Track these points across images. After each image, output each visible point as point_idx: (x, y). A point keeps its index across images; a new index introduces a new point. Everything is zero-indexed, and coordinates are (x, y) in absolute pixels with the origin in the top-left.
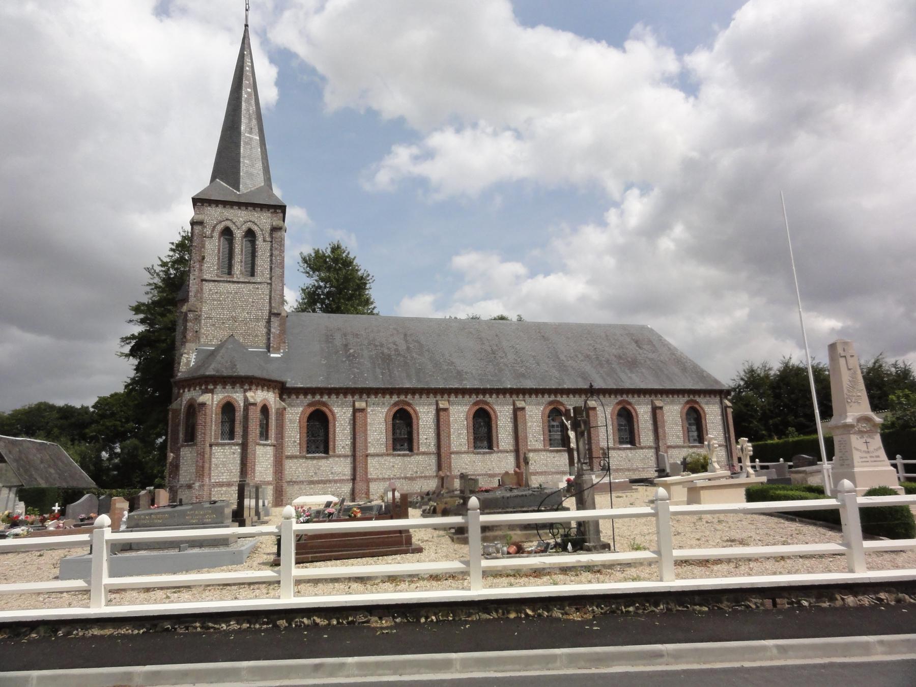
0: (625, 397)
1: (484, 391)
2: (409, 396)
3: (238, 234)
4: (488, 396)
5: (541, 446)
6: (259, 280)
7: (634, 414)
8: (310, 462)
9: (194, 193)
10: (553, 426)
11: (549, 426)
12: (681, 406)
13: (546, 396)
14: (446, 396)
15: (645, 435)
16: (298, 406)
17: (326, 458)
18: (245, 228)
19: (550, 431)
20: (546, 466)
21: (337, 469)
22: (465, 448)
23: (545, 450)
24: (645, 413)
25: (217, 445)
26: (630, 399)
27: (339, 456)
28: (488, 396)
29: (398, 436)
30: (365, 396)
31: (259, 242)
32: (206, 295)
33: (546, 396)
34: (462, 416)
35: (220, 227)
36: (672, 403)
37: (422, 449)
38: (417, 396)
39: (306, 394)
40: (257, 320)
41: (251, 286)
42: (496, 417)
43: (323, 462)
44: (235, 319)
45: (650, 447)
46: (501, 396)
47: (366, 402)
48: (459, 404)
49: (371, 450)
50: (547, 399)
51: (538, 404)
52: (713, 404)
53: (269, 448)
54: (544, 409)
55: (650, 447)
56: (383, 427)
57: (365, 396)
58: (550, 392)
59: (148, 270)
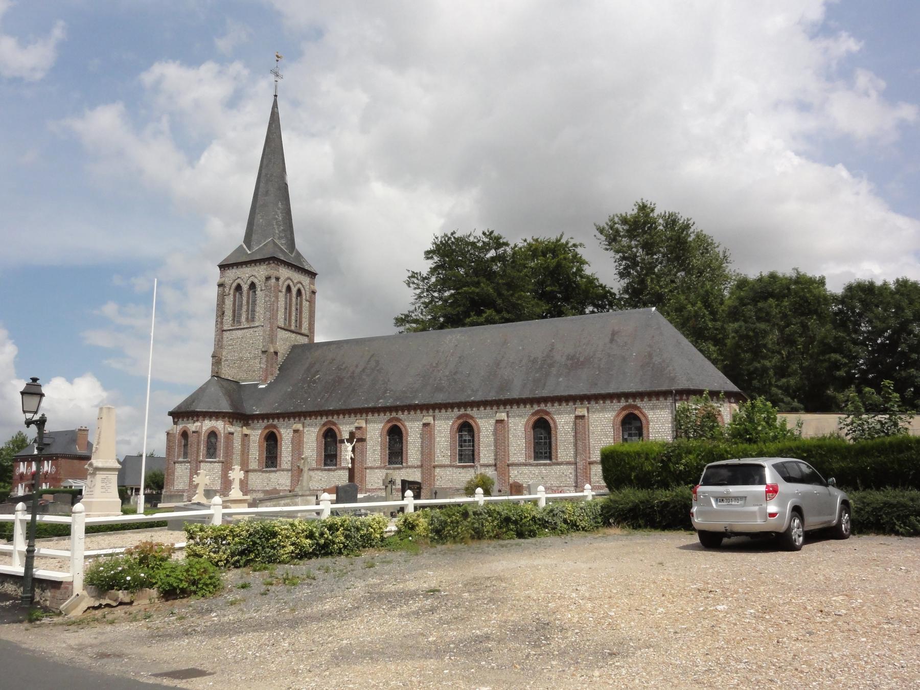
0: (543, 406)
1: (396, 409)
2: (335, 417)
3: (245, 288)
4: (400, 413)
5: (448, 462)
6: (257, 324)
7: (552, 425)
8: (264, 474)
9: (218, 263)
10: (465, 441)
11: (460, 441)
12: (614, 414)
13: (456, 410)
14: (431, 411)
15: (486, 454)
16: (258, 429)
17: (549, 465)
18: (249, 282)
19: (461, 446)
20: (452, 482)
21: (282, 481)
22: (378, 464)
23: (451, 466)
24: (566, 423)
25: (178, 462)
26: (549, 408)
27: (283, 470)
28: (400, 413)
29: (329, 452)
30: (302, 419)
31: (258, 292)
32: (225, 343)
33: (456, 410)
34: (377, 433)
35: (234, 285)
36: (603, 410)
37: (343, 465)
38: (341, 416)
39: (322, 416)
40: (255, 358)
41: (251, 330)
42: (407, 433)
43: (272, 475)
44: (241, 359)
45: (568, 463)
46: (412, 413)
47: (303, 424)
48: (375, 422)
49: (513, 459)
50: (456, 412)
51: (448, 419)
52: (662, 409)
53: (216, 464)
54: (453, 424)
55: (568, 463)
56: (315, 445)
57: (302, 419)
58: (459, 405)
59: (400, 321)
